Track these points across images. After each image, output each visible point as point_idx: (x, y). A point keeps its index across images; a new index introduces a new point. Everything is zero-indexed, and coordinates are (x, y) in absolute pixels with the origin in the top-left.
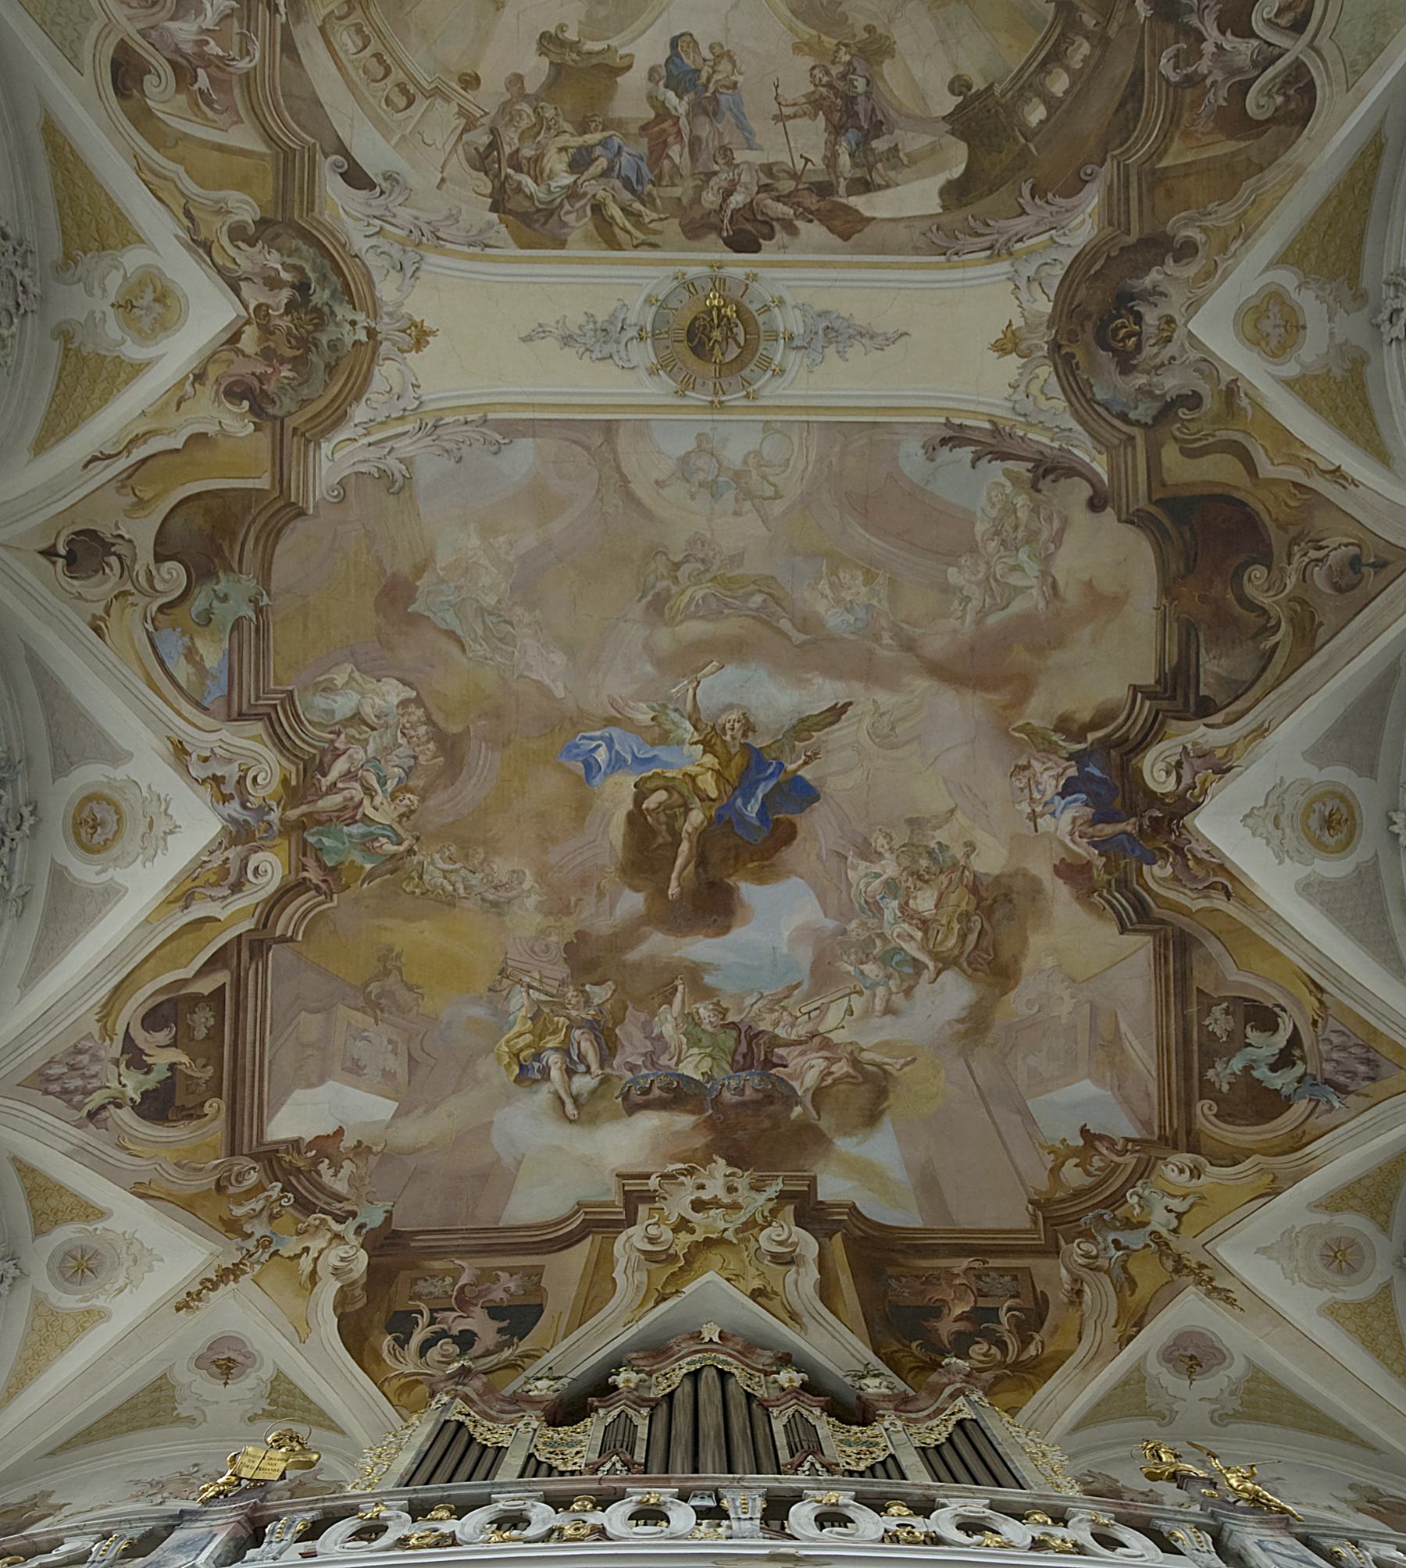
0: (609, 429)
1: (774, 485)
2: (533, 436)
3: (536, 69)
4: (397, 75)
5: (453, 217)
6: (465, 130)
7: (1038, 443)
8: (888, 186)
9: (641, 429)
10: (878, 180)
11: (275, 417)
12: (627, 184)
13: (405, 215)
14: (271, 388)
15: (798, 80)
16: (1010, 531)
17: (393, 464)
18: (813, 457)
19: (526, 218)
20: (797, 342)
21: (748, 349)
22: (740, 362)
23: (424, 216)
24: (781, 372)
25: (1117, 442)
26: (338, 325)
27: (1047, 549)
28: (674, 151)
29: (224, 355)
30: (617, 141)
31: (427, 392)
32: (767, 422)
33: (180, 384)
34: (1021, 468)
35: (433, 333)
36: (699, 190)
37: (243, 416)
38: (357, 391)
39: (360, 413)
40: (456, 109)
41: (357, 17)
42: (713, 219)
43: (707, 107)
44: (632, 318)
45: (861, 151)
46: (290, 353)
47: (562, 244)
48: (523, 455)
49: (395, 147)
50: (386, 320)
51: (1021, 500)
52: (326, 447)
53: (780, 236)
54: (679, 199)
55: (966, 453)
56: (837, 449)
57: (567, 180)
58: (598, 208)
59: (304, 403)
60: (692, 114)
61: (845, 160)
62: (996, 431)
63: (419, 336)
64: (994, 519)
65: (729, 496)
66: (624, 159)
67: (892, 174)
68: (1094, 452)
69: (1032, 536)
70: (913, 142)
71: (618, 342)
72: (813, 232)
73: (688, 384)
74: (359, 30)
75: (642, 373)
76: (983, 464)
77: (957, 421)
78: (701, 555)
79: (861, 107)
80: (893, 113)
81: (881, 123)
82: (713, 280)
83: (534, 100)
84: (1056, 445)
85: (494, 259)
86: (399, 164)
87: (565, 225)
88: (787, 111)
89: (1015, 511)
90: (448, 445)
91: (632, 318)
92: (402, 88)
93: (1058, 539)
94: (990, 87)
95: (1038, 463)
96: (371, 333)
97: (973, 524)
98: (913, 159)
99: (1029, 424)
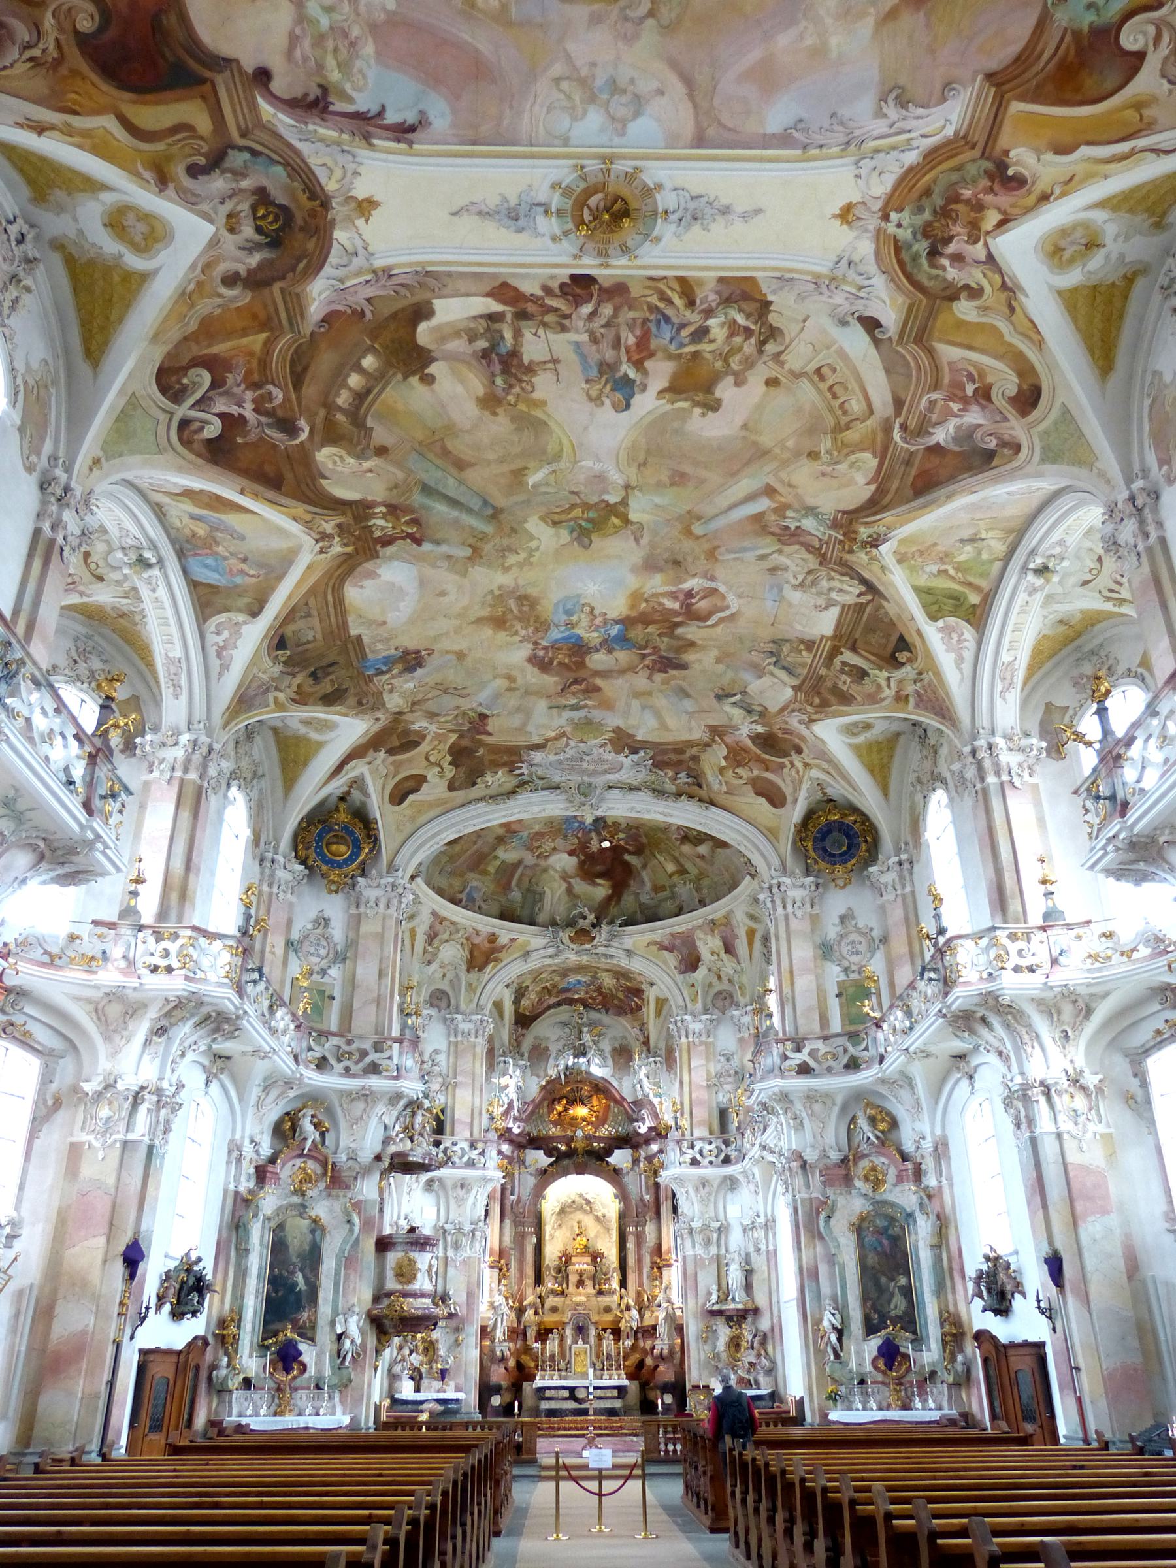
0: (700, 141)
1: (561, 91)
2: (765, 135)
3: (725, 390)
4: (824, 386)
5: (801, 297)
6: (781, 353)
7: (327, 128)
8: (475, 318)
9: (673, 140)
10: (483, 322)
11: (988, 159)
12: (667, 319)
13: (839, 299)
14: (985, 183)
15: (543, 385)
16: (340, 46)
17: (892, 112)
18: (526, 118)
19: (746, 297)
20: (541, 209)
21: (581, 203)
22: (589, 192)
23: (823, 298)
24: (555, 186)
25: (257, 132)
26: (912, 226)
27: (303, 29)
28: (631, 340)
29: (1016, 211)
30: (672, 347)
31: (851, 171)
32: (566, 142)
33: (1064, 194)
34: (339, 106)
35: (835, 216)
36: (615, 315)
37: (1017, 163)
38: (910, 175)
39: (911, 158)
40: (787, 366)
41: (844, 420)
42: (605, 296)
43: (606, 368)
44: (673, 227)
45: (496, 340)
46: (960, 207)
47: (721, 280)
48: (776, 118)
49: (834, 342)
50: (871, 228)
51: (335, 76)
52: (949, 132)
53: (555, 285)
54: (630, 309)
55: (391, 118)
56: (505, 122)
57: (711, 322)
58: (691, 304)
59: (958, 168)
60: (618, 363)
61: (508, 335)
62: (367, 138)
63: (847, 214)
64: (358, 57)
65: (599, 82)
66: (668, 336)
67: (472, 325)
68: (275, 121)
69: (319, 40)
70: (458, 345)
71: (686, 209)
72: (530, 287)
73: (631, 177)
74: (845, 413)
75: (668, 185)
76: (375, 109)
77: (403, 146)
78: (628, 25)
79: (498, 368)
80: (474, 362)
81: (483, 357)
82: (607, 255)
83: (728, 370)
84: (311, 127)
85: (775, 269)
86: (836, 332)
87: (718, 293)
88: (551, 366)
89: (339, 65)
90: (841, 128)
91: (673, 227)
92: (822, 378)
93: (294, 40)
94: (405, 378)
95: (325, 110)
96: (886, 217)
97: (378, 53)
98: (457, 334)
99: (338, 144)
